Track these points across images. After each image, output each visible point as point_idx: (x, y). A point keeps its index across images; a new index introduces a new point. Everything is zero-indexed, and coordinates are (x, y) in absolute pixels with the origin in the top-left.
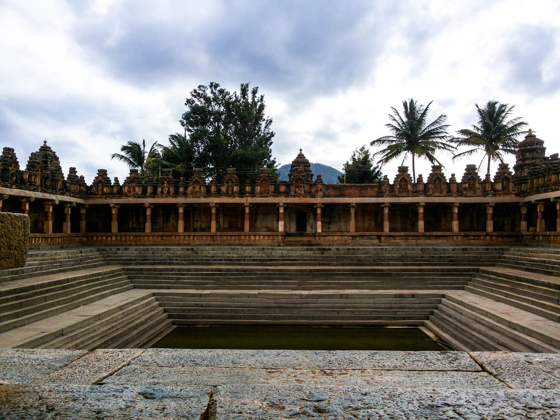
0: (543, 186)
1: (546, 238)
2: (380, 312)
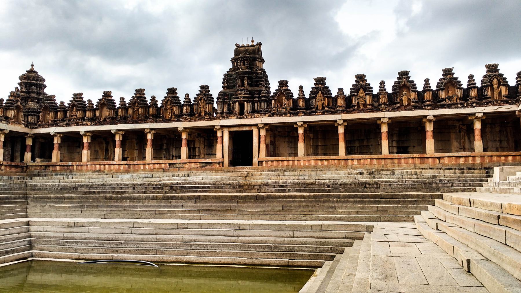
0: (63, 120)
1: (66, 168)
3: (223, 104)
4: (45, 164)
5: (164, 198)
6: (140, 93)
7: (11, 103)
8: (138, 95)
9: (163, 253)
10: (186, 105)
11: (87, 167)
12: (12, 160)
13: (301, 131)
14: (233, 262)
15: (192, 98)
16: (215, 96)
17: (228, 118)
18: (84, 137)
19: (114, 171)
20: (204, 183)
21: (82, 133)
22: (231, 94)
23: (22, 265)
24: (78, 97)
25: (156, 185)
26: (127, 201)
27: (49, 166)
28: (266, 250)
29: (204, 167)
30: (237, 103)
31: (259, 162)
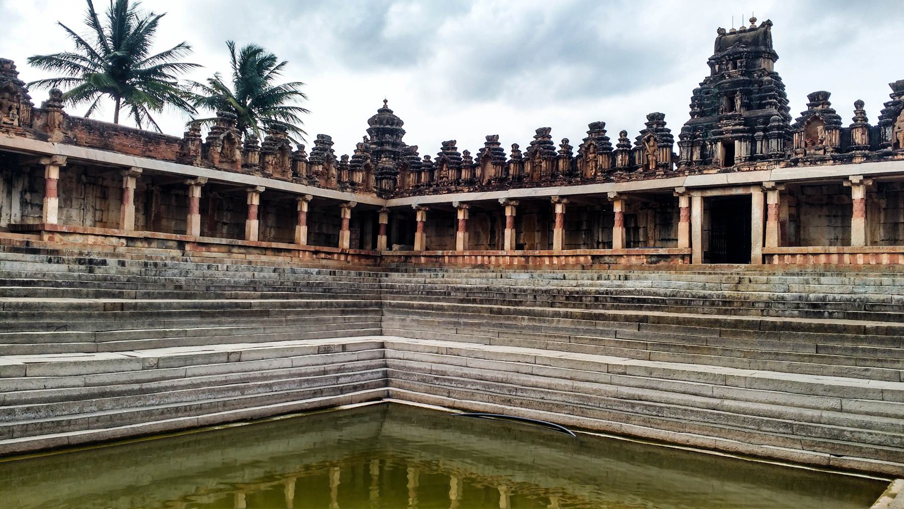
0: (429, 185)
1: (434, 259)
2: (314, 381)
3: (692, 147)
4: (405, 253)
5: (583, 316)
6: (543, 134)
7: (359, 162)
8: (540, 139)
9: (583, 414)
10: (622, 152)
11: (464, 260)
12: (361, 247)
13: (858, 194)
15: (632, 139)
16: (676, 133)
17: (701, 172)
19: (503, 266)
20: (655, 294)
21: (455, 205)
22: (707, 126)
23: (375, 408)
24: (449, 146)
25: (571, 293)
26: (523, 319)
27: (410, 257)
28: (781, 430)
29: (655, 263)
30: (719, 144)
31: (764, 255)
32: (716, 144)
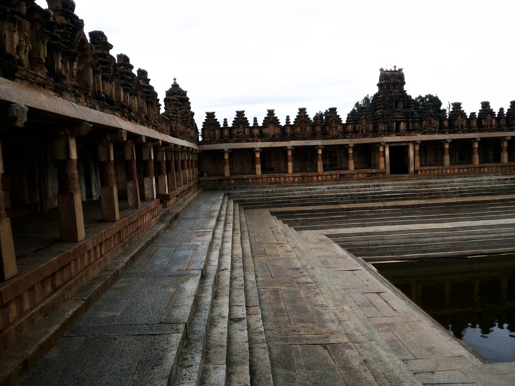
0: (231, 137)
1: (240, 181)
5: (393, 207)
14: (512, 250)
18: (256, 154)
20: (398, 192)
24: (240, 114)
25: (358, 195)
27: (223, 180)
32: (393, 123)
